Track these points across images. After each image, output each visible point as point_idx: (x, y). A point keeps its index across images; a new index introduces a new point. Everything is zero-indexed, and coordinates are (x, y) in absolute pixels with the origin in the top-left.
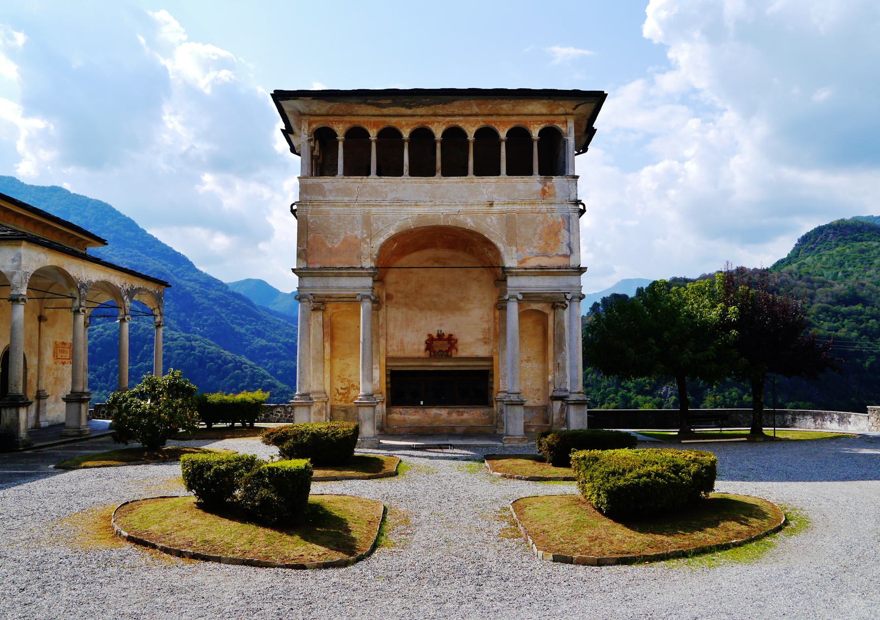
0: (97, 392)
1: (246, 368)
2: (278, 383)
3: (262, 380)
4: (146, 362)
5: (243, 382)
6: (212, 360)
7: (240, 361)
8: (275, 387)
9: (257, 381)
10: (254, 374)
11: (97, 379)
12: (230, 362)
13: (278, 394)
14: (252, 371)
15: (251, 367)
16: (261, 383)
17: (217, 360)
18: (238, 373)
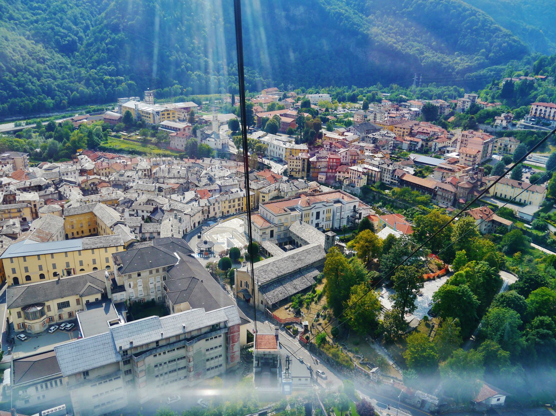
0: (376, 27)
1: (479, 15)
2: (502, 28)
3: (491, 25)
4: (408, 8)
5: (477, 25)
6: (455, 8)
7: (475, 10)
8: (501, 31)
9: (487, 26)
10: (485, 20)
11: (376, 20)
12: (468, 10)
13: (502, 36)
14: (483, 18)
15: (483, 15)
16: (490, 27)
17: (458, 8)
18: (473, 19)
